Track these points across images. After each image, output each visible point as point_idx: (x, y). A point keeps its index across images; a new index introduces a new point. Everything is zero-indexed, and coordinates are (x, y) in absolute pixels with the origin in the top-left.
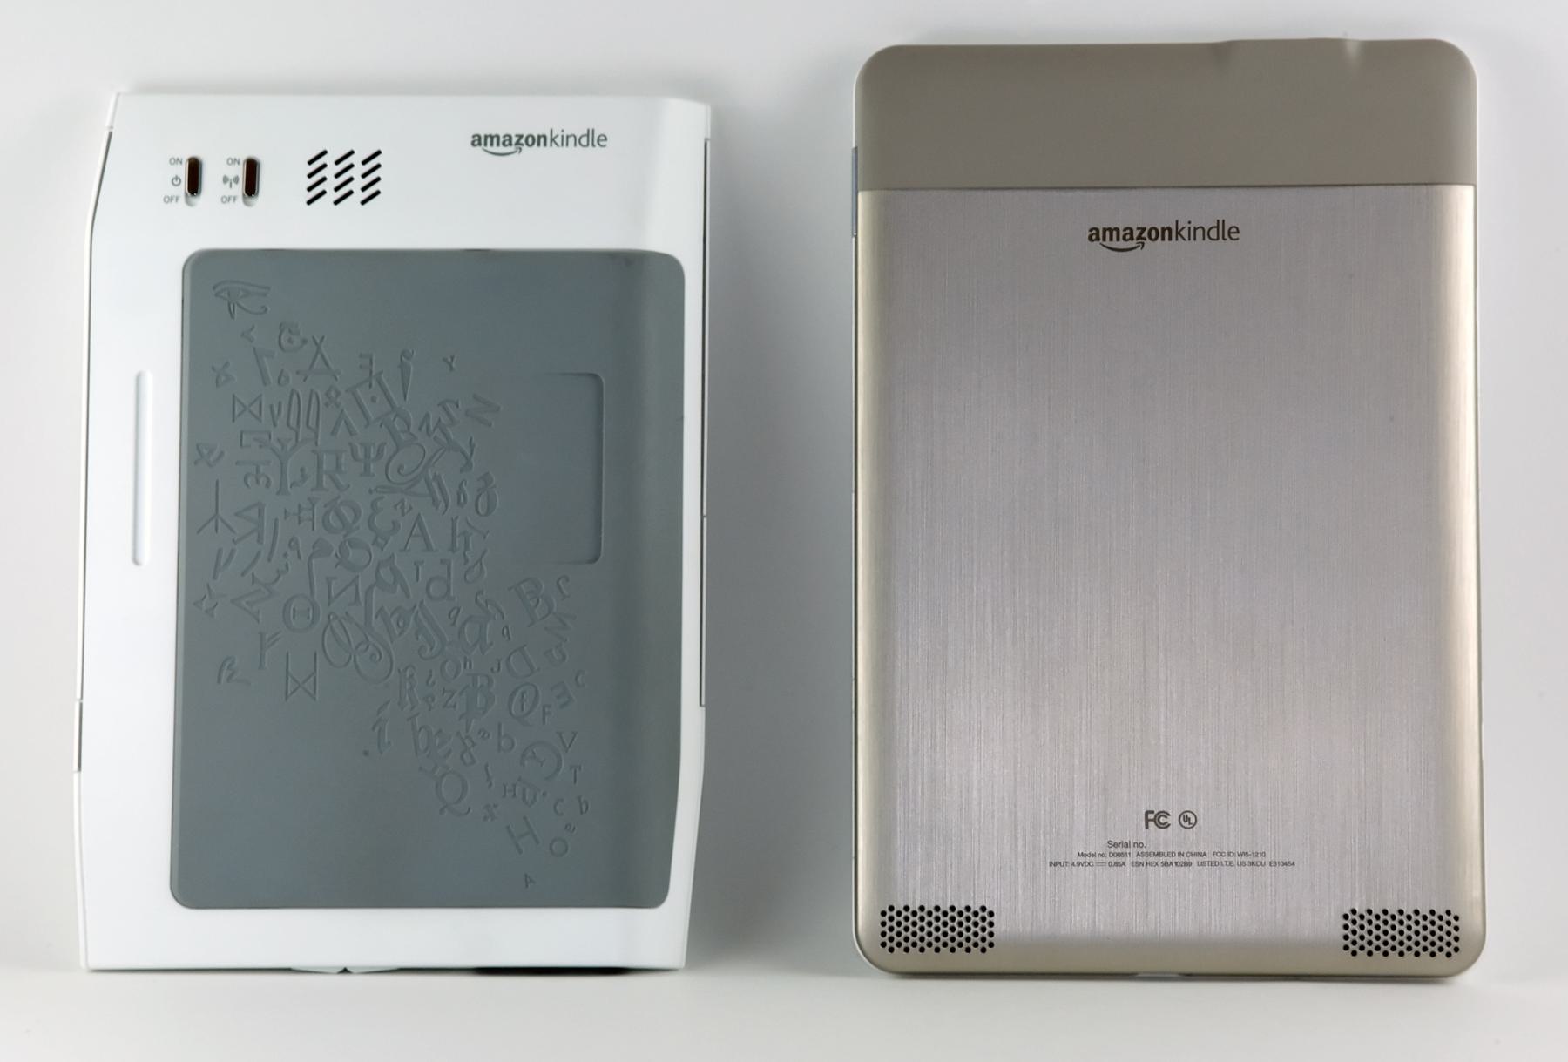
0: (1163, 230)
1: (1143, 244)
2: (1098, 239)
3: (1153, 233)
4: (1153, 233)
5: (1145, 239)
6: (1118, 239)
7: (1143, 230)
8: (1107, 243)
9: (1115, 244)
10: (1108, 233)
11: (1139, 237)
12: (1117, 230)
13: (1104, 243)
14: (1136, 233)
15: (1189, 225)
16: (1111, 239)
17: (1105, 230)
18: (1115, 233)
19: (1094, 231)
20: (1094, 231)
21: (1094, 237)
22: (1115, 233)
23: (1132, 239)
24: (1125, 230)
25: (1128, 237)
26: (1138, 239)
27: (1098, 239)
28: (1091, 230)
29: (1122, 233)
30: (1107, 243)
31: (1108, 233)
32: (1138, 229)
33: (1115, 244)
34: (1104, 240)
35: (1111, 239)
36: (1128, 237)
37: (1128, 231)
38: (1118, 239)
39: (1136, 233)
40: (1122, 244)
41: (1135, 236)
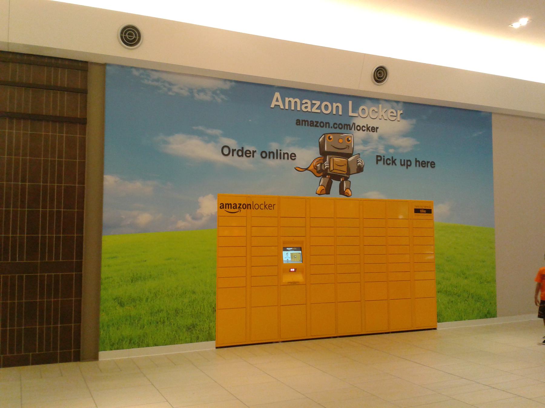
0: (248, 205)
1: (240, 210)
2: (223, 208)
3: (244, 206)
4: (244, 206)
5: (241, 208)
6: (231, 208)
7: (240, 204)
8: (227, 210)
9: (230, 210)
10: (227, 205)
11: (239, 208)
14: (238, 206)
16: (228, 208)
18: (230, 205)
19: (222, 205)
20: (222, 205)
21: (222, 207)
22: (230, 205)
23: (236, 208)
24: (234, 204)
25: (235, 207)
27: (223, 208)
28: (221, 204)
29: (232, 206)
30: (227, 210)
31: (227, 205)
32: (239, 204)
33: (230, 210)
34: (226, 208)
35: (228, 208)
37: (235, 205)
38: (231, 208)
39: (238, 206)
41: (238, 207)
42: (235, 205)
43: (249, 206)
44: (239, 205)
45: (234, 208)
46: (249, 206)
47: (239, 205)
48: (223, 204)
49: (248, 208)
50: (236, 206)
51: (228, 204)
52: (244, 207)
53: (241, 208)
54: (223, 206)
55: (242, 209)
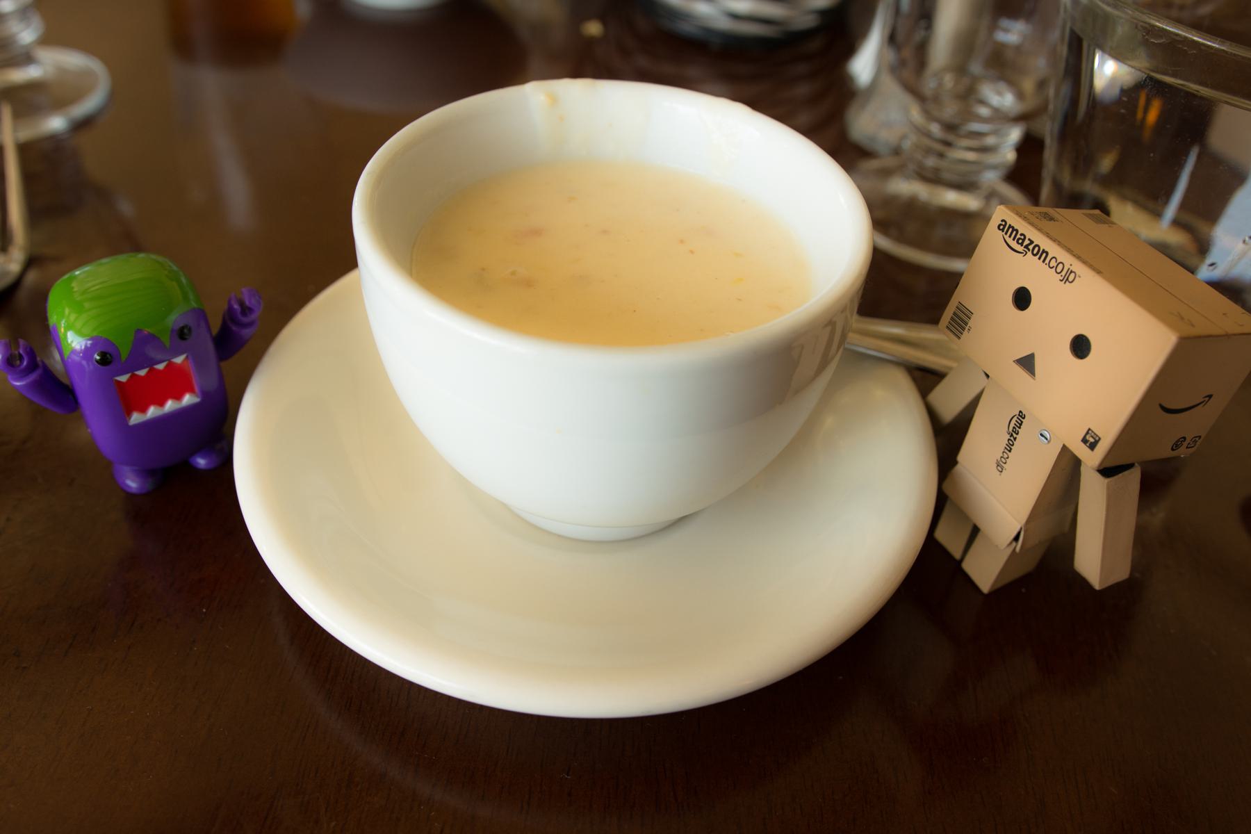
1: (1026, 253)
2: (1003, 230)
3: (1037, 249)
4: (1037, 249)
5: (1029, 250)
6: (1014, 239)
7: (1032, 242)
8: (1007, 237)
9: (1010, 241)
10: (1011, 230)
11: (1026, 247)
12: (1017, 231)
13: (1005, 235)
14: (1027, 242)
15: (1070, 267)
16: (1010, 237)
17: (1010, 226)
18: (1015, 232)
20: (1004, 223)
21: (1001, 227)
23: (1022, 244)
25: (1020, 241)
26: (1025, 247)
28: (1002, 221)
29: (1018, 236)
30: (1007, 237)
31: (1011, 230)
32: (1029, 239)
33: (1010, 241)
34: (1006, 234)
35: (1010, 237)
36: (1020, 241)
37: (1022, 237)
39: (1027, 242)
40: (1014, 244)
41: (1025, 243)
42: (1022, 237)
43: (1044, 255)
44: (1029, 242)
45: (1018, 242)
46: (1044, 255)
47: (1029, 242)
48: (1006, 223)
49: (1039, 258)
50: (1024, 240)
51: (1013, 227)
52: (1035, 252)
53: (1029, 250)
54: (1005, 226)
55: (1029, 253)
